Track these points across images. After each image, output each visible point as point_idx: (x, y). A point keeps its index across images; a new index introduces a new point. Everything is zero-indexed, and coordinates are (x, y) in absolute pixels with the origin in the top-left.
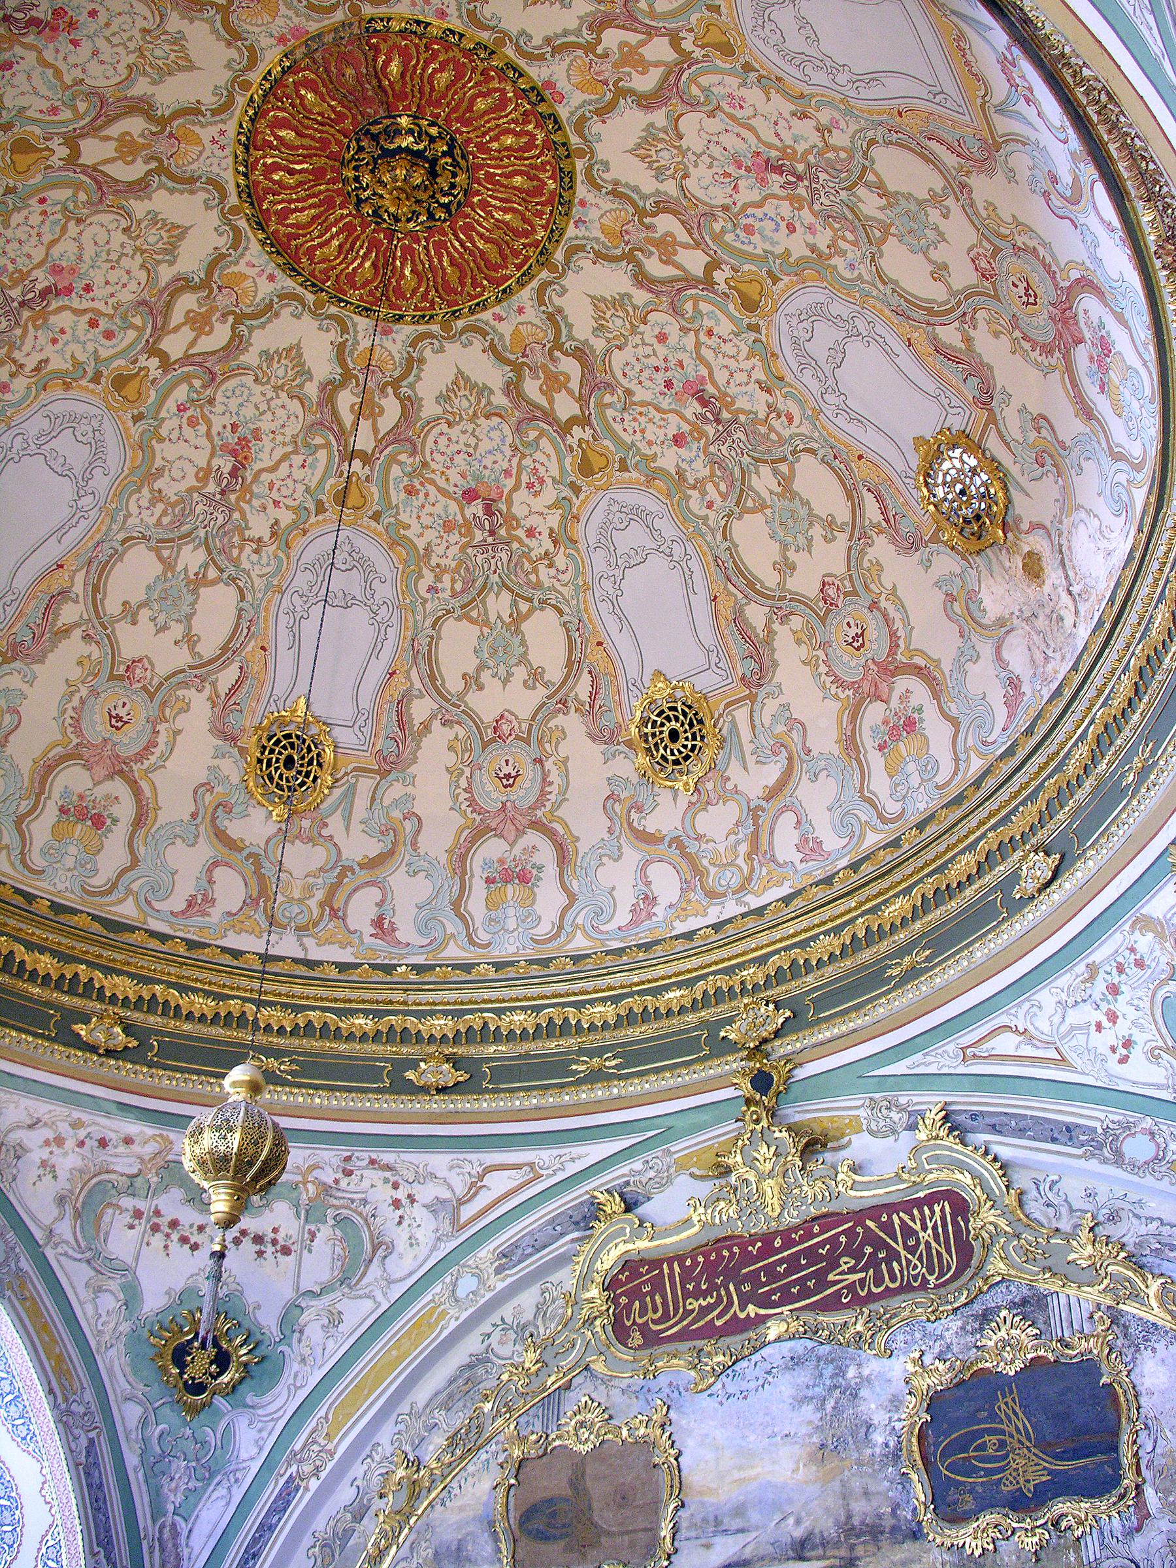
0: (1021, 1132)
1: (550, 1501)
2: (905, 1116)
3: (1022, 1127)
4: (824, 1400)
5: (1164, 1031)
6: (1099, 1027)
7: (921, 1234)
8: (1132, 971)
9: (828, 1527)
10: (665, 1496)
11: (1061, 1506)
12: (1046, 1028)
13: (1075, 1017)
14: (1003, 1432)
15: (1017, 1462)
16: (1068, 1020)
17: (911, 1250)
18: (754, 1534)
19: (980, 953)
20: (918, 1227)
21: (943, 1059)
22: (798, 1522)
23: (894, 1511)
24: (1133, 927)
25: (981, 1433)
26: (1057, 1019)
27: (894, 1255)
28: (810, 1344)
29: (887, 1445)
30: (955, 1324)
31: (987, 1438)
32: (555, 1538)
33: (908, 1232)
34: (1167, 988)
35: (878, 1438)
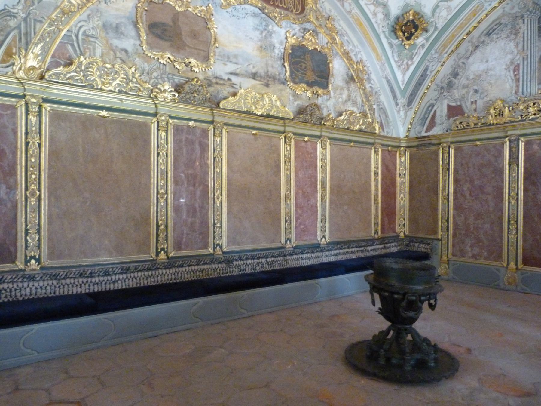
1: (163, 24)
4: (262, 32)
9: (262, 72)
10: (213, 43)
11: (318, 89)
15: (309, 72)
18: (239, 66)
22: (254, 67)
23: (279, 74)
25: (301, 62)
28: (260, 12)
29: (278, 54)
30: (298, 28)
31: (302, 64)
32: (166, 40)
35: (277, 51)
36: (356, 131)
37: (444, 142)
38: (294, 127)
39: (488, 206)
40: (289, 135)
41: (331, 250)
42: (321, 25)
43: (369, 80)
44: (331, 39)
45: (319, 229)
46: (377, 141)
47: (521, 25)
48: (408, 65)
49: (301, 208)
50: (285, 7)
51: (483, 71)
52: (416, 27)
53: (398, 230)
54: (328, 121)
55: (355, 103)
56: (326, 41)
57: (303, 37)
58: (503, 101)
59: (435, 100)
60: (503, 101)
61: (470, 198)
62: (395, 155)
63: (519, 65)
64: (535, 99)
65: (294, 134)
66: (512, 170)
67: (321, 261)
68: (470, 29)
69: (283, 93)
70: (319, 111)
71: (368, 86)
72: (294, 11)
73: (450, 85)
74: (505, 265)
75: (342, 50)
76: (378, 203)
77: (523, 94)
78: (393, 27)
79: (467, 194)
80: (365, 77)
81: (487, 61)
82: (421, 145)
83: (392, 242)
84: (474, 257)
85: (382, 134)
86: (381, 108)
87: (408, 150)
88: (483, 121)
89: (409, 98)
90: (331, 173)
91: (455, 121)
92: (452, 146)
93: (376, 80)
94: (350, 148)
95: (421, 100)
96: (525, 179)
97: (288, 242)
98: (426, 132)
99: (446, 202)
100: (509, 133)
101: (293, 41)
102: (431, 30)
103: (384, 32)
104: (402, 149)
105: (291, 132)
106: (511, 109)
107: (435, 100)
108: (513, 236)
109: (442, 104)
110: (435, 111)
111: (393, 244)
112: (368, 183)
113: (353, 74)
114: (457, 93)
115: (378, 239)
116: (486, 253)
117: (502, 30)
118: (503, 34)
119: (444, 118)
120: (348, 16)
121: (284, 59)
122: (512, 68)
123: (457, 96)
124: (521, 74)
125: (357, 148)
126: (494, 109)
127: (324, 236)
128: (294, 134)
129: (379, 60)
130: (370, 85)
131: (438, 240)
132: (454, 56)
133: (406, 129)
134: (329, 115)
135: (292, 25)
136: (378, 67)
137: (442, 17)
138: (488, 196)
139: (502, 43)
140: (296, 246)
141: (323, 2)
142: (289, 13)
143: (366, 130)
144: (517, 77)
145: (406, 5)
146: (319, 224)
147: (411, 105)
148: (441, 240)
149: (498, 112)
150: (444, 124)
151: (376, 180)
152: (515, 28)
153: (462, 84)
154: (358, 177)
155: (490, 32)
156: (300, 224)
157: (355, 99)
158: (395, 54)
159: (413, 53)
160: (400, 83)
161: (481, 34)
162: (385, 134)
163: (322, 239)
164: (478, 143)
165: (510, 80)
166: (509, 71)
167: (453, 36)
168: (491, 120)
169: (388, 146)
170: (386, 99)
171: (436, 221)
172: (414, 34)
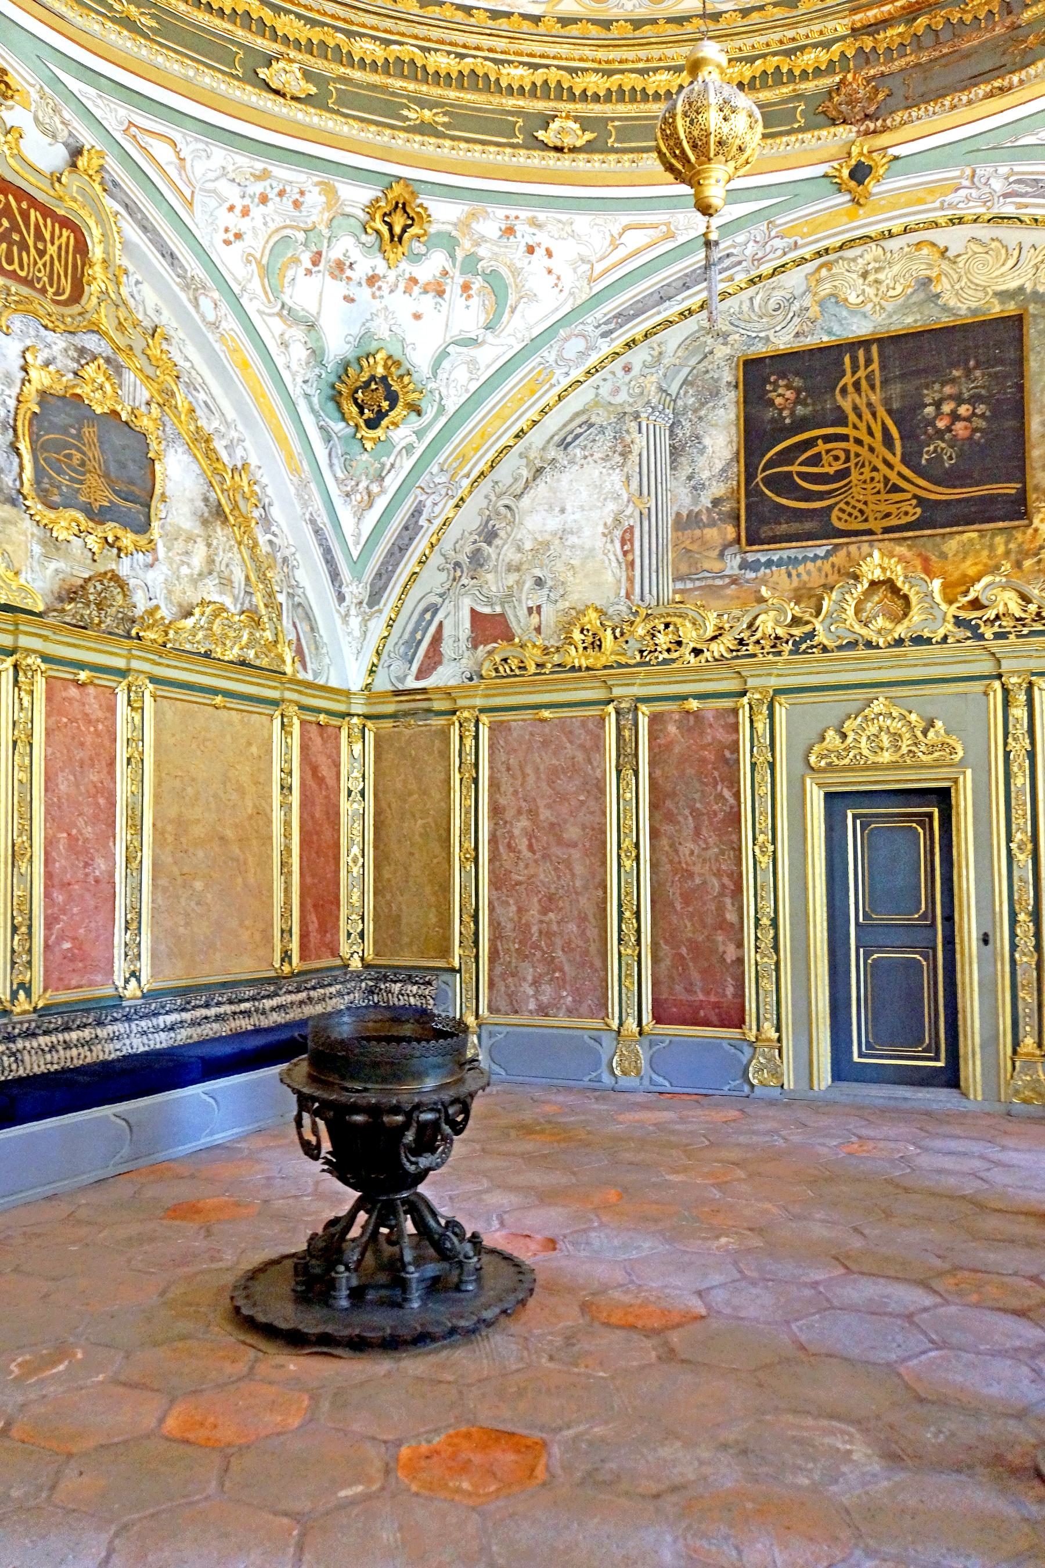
0: (145, 229)
2: (66, 133)
3: (146, 227)
5: (267, 252)
6: (231, 208)
7: (49, 245)
8: (287, 203)
11: (120, 533)
12: (198, 173)
13: (224, 187)
14: (84, 454)
15: (92, 480)
16: (216, 184)
17: (41, 253)
19: (208, 80)
20: (48, 236)
21: (115, 115)
24: (317, 184)
25: (67, 446)
26: (211, 175)
27: (23, 246)
31: (73, 452)
33: (39, 236)
34: (296, 233)
36: (232, 662)
37: (465, 708)
38: (45, 638)
39: (573, 875)
40: (30, 661)
41: (156, 1014)
42: (131, 348)
43: (266, 521)
44: (161, 391)
45: (118, 952)
46: (288, 695)
47: (635, 435)
48: (369, 494)
49: (66, 885)
50: (23, 274)
51: (554, 534)
52: (393, 399)
53: (344, 949)
54: (149, 627)
55: (226, 583)
56: (146, 395)
57: (76, 374)
58: (601, 612)
59: (441, 595)
60: (601, 612)
61: (530, 854)
62: (338, 738)
63: (631, 528)
64: (668, 615)
65: (46, 659)
66: (623, 784)
67: (126, 1050)
68: (523, 423)
69: (11, 530)
70: (125, 596)
71: (262, 539)
72: (51, 291)
73: (477, 559)
74: (615, 1025)
75: (192, 428)
76: (290, 873)
77: (642, 600)
78: (333, 387)
79: (523, 844)
80: (256, 513)
81: (563, 511)
82: (406, 714)
83: (330, 985)
84: (543, 1010)
85: (301, 676)
86: (300, 604)
87: (369, 724)
88: (556, 659)
89: (372, 585)
90: (158, 784)
91: (490, 653)
92: (484, 718)
93: (288, 525)
94: (211, 709)
95: (405, 590)
96: (654, 806)
97: (22, 994)
98: (417, 678)
99: (470, 866)
100: (617, 692)
101: (47, 382)
102: (430, 412)
103: (307, 396)
104: (355, 720)
105: (34, 652)
106: (618, 634)
107: (441, 595)
108: (629, 951)
109: (457, 607)
110: (441, 623)
111: (333, 990)
112: (263, 814)
113: (223, 501)
114: (494, 583)
115: (293, 975)
116: (570, 999)
117: (594, 440)
118: (595, 449)
119: (463, 644)
120: (210, 336)
121: (15, 430)
122: (618, 533)
123: (494, 589)
124: (637, 552)
125: (233, 713)
126: (582, 632)
127: (133, 974)
128: (46, 659)
129: (295, 471)
130: (269, 537)
131: (453, 970)
132: (486, 485)
133: (366, 666)
134: (151, 612)
135: (43, 332)
136: (293, 490)
137: (455, 386)
138: (572, 851)
139: (594, 471)
140: (46, 1007)
141: (137, 283)
142: (34, 294)
143: (257, 663)
144: (630, 557)
145: (367, 335)
146: (120, 937)
147: (378, 603)
148: (459, 971)
149: (591, 640)
150: (464, 661)
151: (286, 806)
152: (622, 439)
153: (507, 560)
154: (235, 796)
155: (569, 439)
156: (61, 938)
157: (227, 573)
158: (335, 461)
159: (383, 465)
160: (350, 541)
161: (548, 442)
162: (309, 677)
163: (127, 981)
164: (546, 714)
165: (614, 564)
166: (612, 541)
167: (484, 436)
168: (575, 657)
169: (319, 711)
170: (310, 578)
171: (446, 922)
172: (386, 414)
